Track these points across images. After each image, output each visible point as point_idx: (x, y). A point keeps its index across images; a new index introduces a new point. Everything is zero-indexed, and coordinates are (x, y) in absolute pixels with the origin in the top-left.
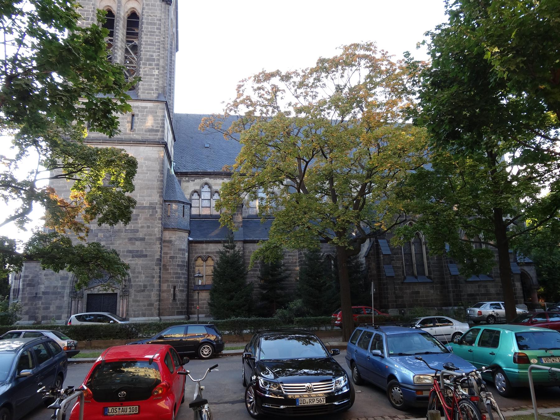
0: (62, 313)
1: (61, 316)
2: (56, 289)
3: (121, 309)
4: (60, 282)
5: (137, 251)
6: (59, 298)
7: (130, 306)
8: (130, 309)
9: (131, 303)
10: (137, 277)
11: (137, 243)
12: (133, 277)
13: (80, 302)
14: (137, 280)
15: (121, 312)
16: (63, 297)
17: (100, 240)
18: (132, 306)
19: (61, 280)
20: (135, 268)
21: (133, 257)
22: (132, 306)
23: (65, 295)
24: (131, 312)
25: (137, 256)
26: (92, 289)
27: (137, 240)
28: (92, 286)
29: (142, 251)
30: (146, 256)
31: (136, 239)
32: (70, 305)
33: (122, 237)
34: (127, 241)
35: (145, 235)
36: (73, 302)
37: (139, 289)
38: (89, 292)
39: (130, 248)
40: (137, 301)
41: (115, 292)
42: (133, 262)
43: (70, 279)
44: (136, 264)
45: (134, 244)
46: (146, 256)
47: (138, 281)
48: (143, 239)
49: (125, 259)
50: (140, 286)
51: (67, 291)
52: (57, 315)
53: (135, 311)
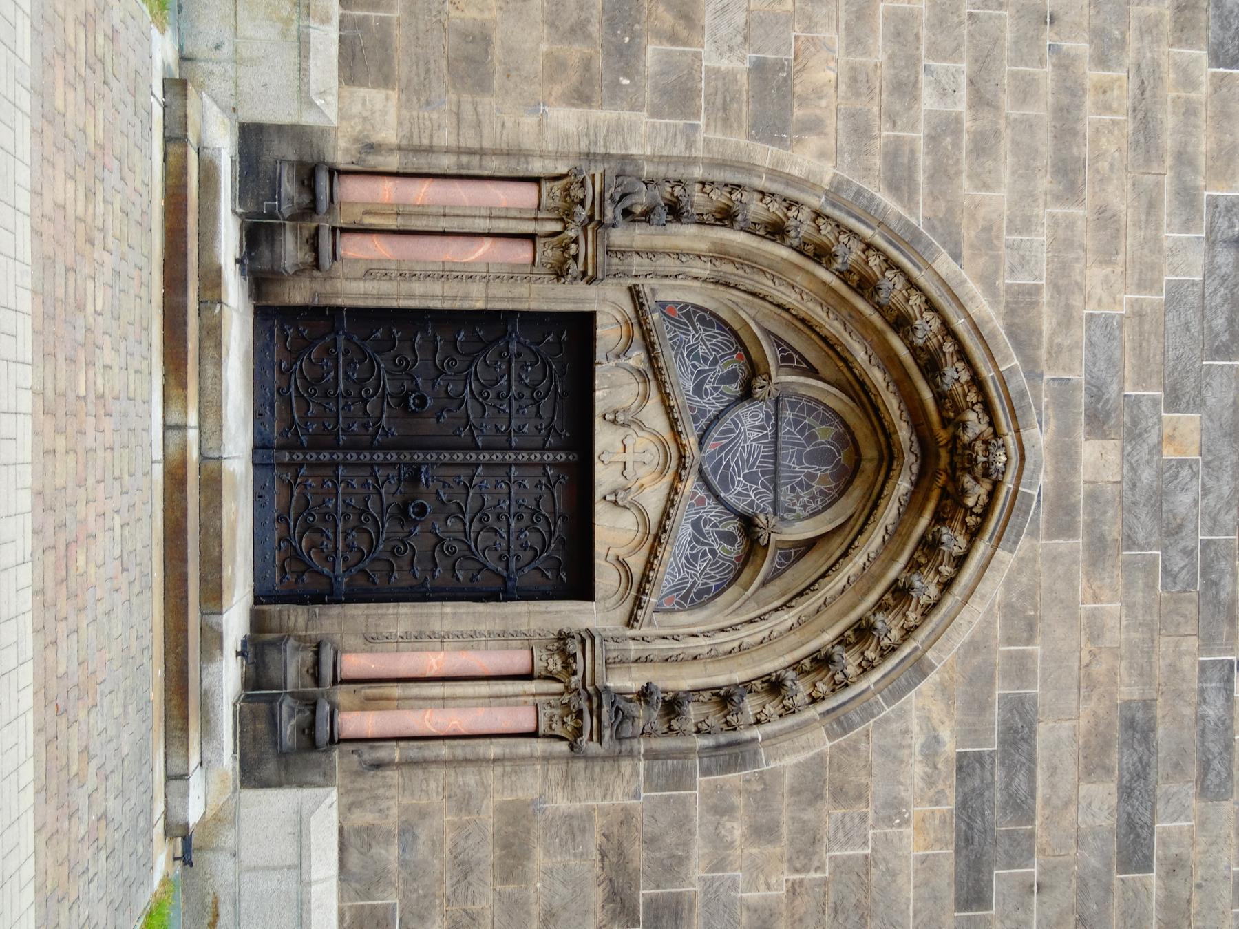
0: (418, 93)
1: (385, 80)
2: (665, 18)
3: (434, 661)
4: (737, 64)
5: (1021, 807)
6: (575, 52)
7: (470, 778)
8: (434, 789)
9: (495, 791)
10: (763, 832)
11: (1099, 802)
12: (768, 783)
13: (521, 253)
14: (736, 830)
15: (406, 663)
16: (581, 97)
17: (1133, 435)
18: (464, 803)
19: (760, 69)
20: (860, 795)
21: (965, 765)
22: (464, 803)
23: (602, 116)
24: (395, 796)
25: (969, 811)
26: (637, 357)
27: (1126, 792)
28: (667, 355)
29: (1021, 849)
30: (973, 895)
31: (1136, 788)
32: (494, 166)
33: (1164, 644)
34: (1128, 691)
35: (1175, 867)
36: (525, 195)
37: (638, 855)
38: (608, 334)
39: (1054, 737)
40: (513, 856)
41: (606, 578)
42: (917, 769)
43: (765, 155)
44: (894, 809)
45: (1092, 768)
46: (973, 895)
47: (718, 842)
48: (1134, 847)
49: (943, 688)
50: (674, 866)
51: (642, 135)
52: (399, 37)
53: (407, 832)
